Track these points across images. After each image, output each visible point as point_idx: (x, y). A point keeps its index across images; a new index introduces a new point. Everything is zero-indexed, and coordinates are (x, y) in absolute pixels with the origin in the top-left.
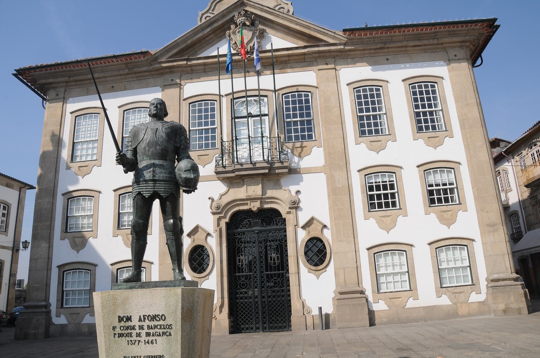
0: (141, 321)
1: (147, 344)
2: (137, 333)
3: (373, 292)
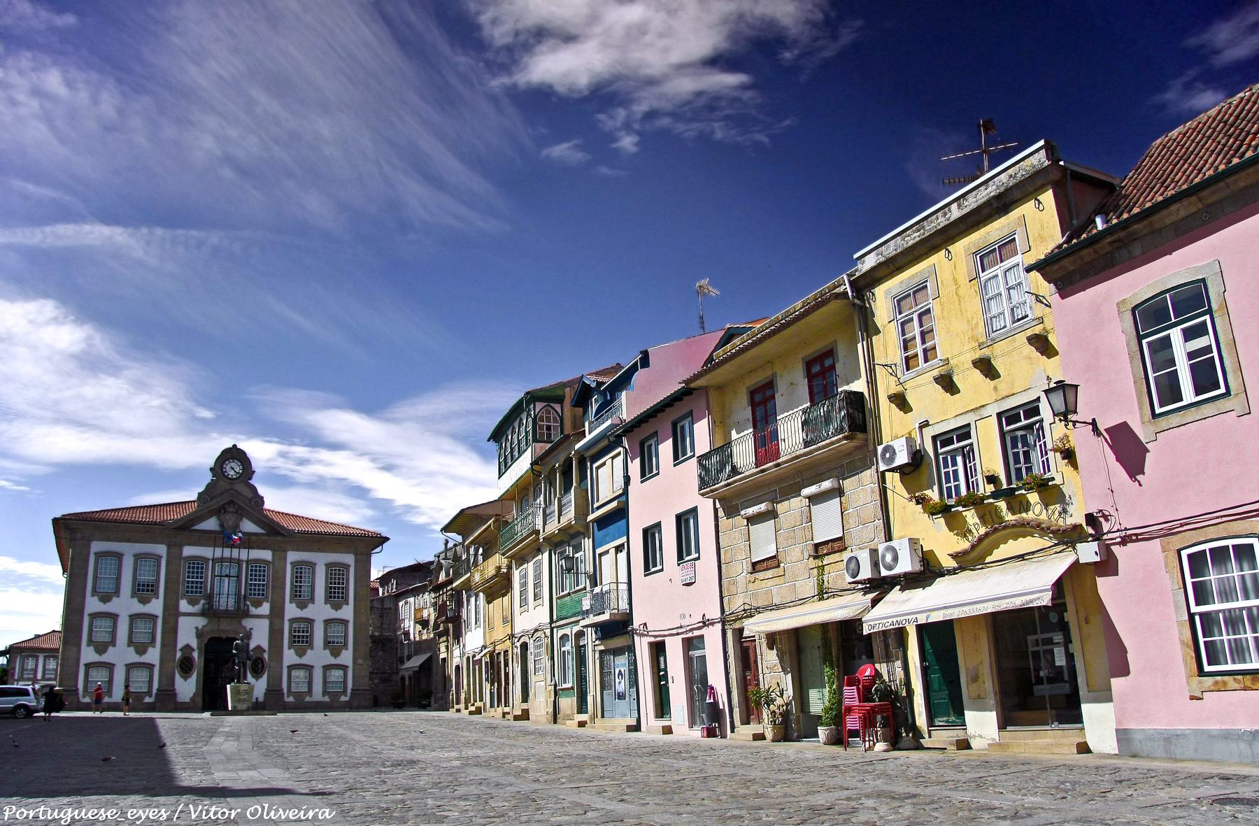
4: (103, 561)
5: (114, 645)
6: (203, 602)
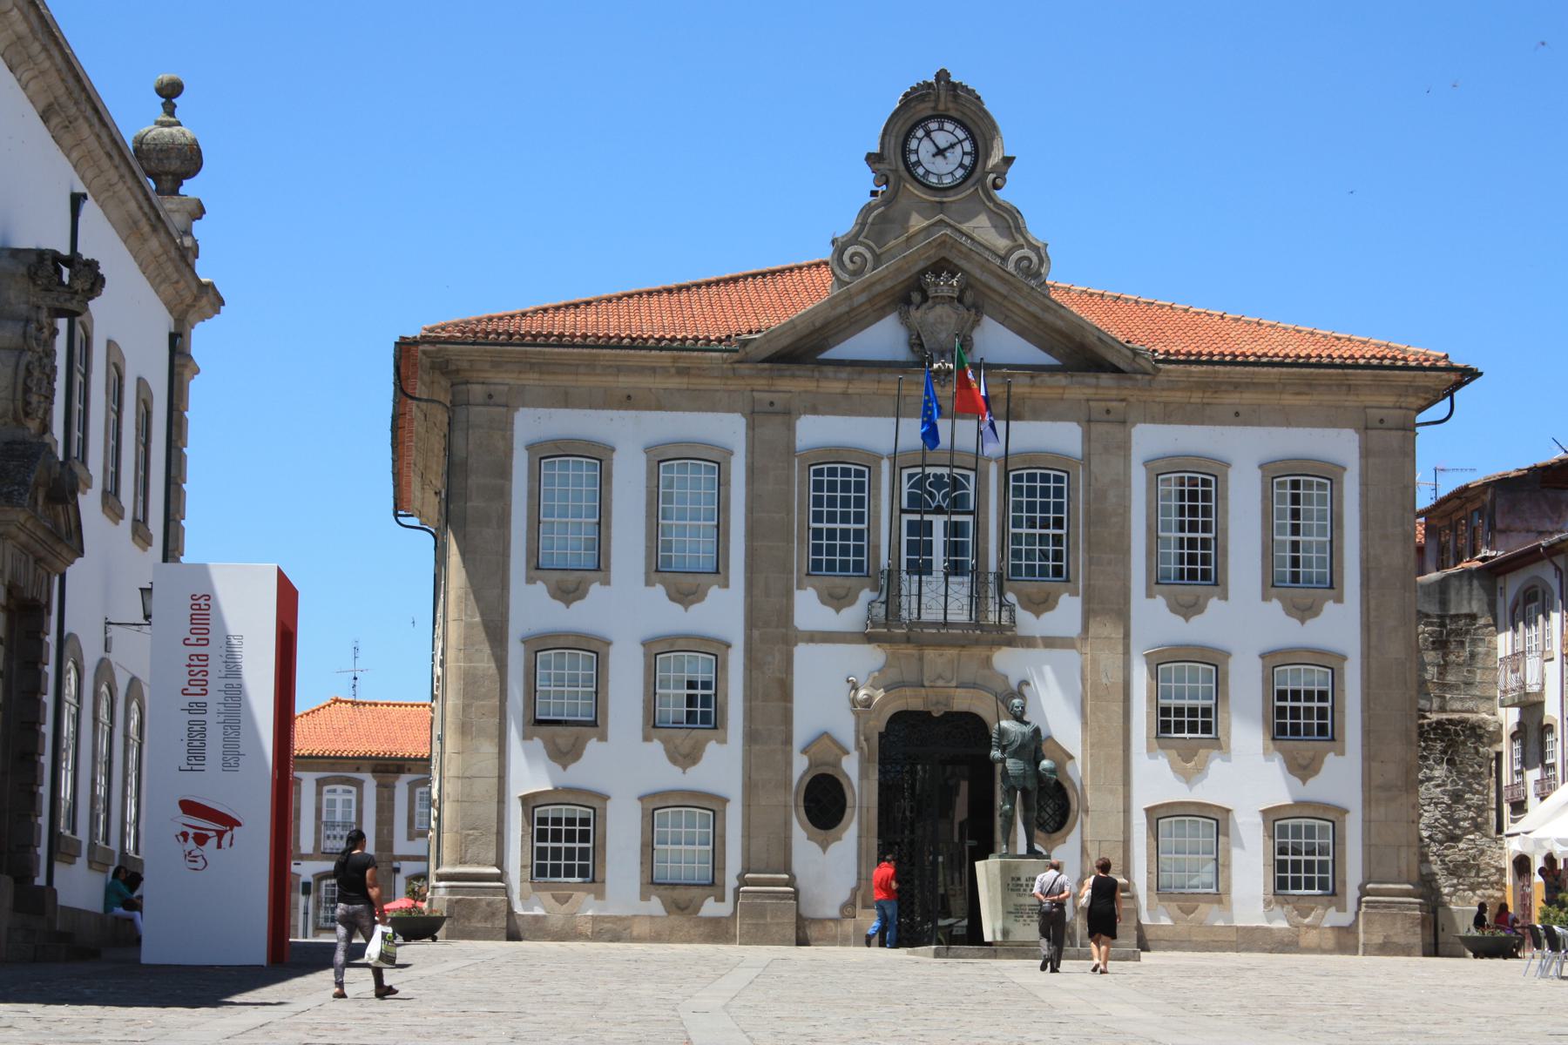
3: (1149, 888)
4: (554, 471)
5: (603, 737)
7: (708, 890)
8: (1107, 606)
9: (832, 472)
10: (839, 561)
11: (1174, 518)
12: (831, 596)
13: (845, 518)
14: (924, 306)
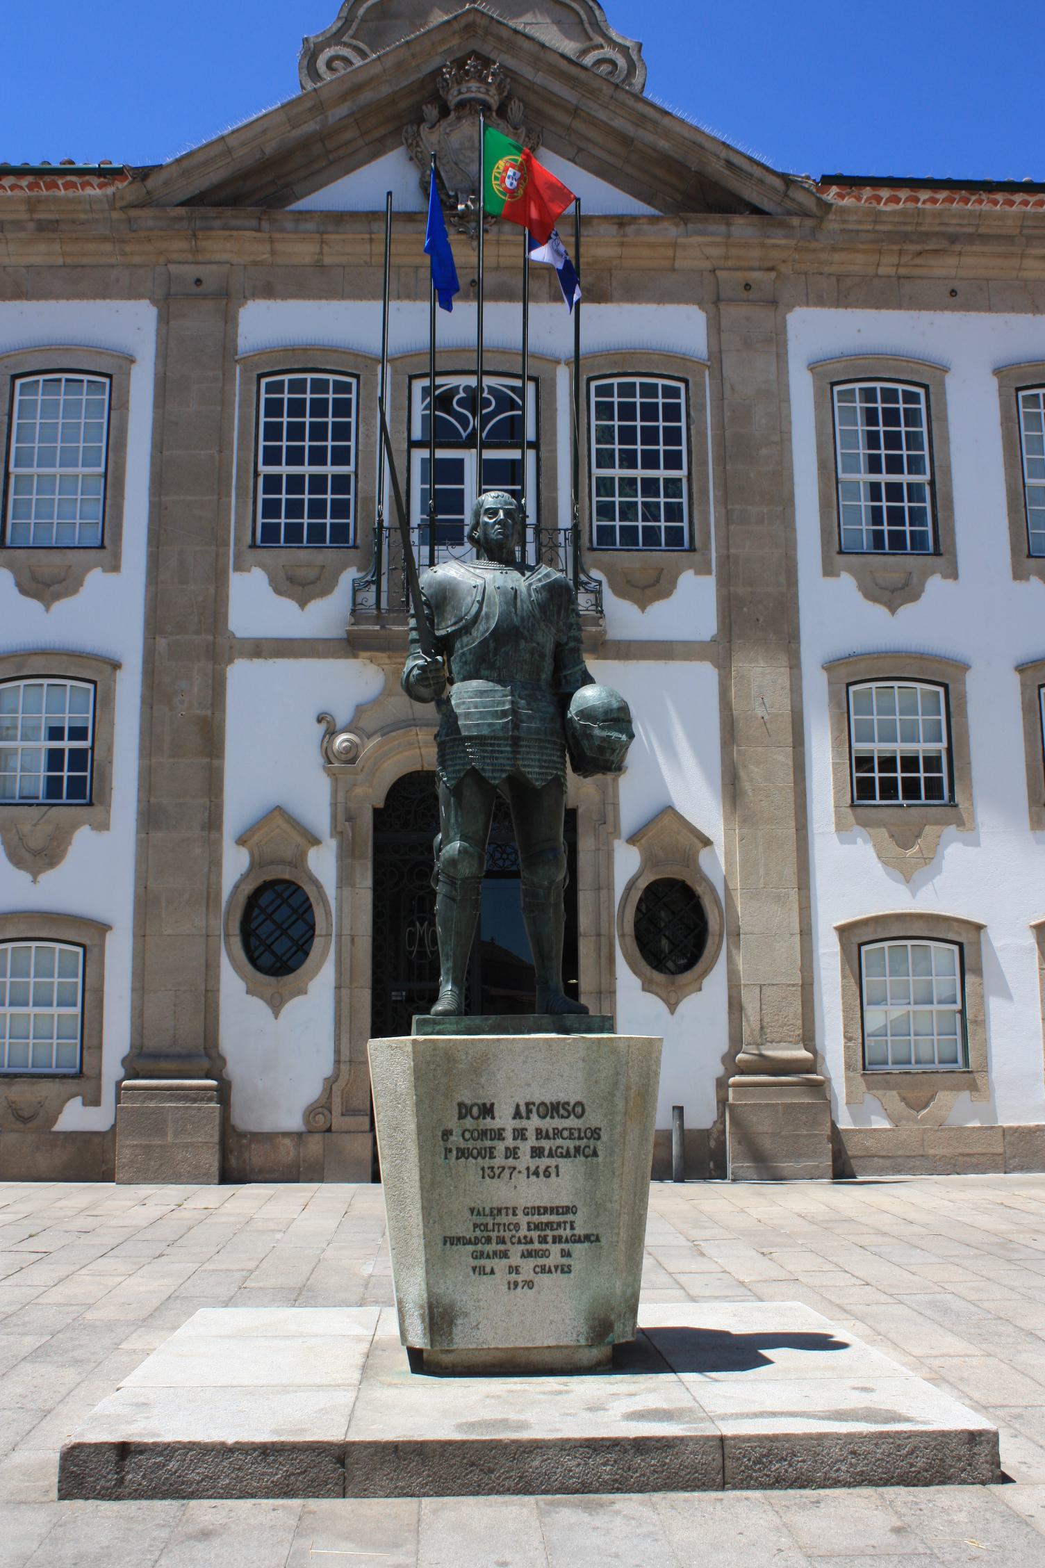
0: (521, 1117)
1: (533, 1178)
2: (507, 1149)
3: (848, 1066)
6: (349, 576)
7: (71, 1085)
8: (759, 616)
9: (297, 386)
10: (301, 526)
11: (863, 451)
12: (291, 580)
13: (318, 457)
14: (444, 123)
